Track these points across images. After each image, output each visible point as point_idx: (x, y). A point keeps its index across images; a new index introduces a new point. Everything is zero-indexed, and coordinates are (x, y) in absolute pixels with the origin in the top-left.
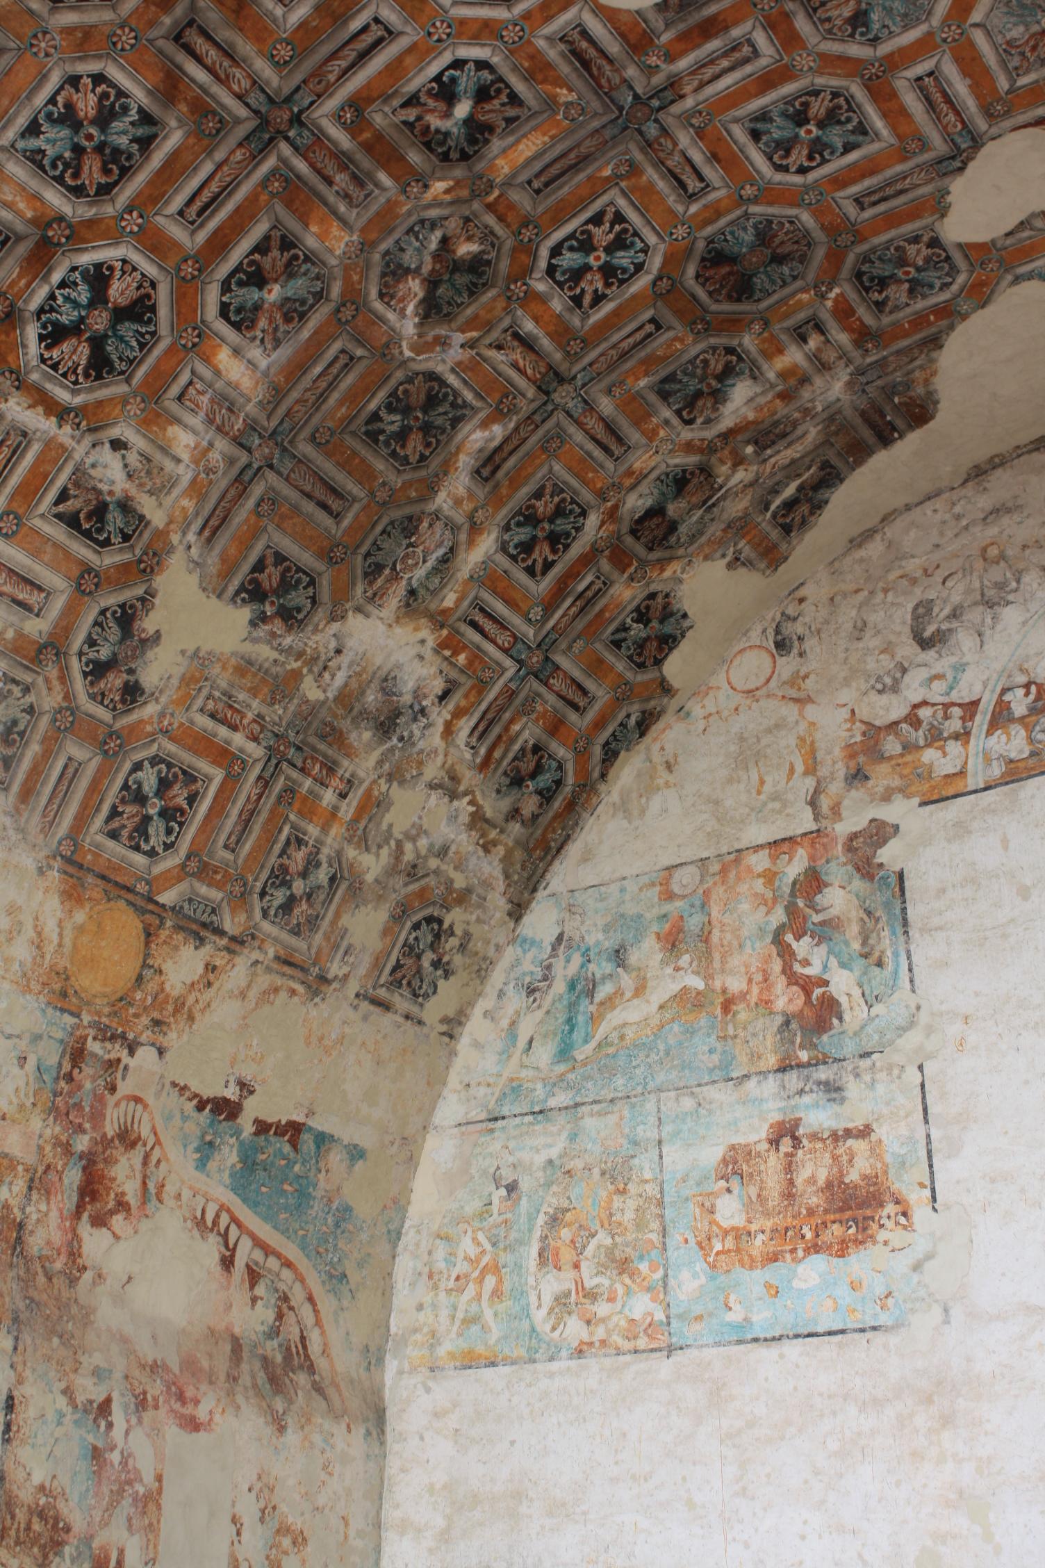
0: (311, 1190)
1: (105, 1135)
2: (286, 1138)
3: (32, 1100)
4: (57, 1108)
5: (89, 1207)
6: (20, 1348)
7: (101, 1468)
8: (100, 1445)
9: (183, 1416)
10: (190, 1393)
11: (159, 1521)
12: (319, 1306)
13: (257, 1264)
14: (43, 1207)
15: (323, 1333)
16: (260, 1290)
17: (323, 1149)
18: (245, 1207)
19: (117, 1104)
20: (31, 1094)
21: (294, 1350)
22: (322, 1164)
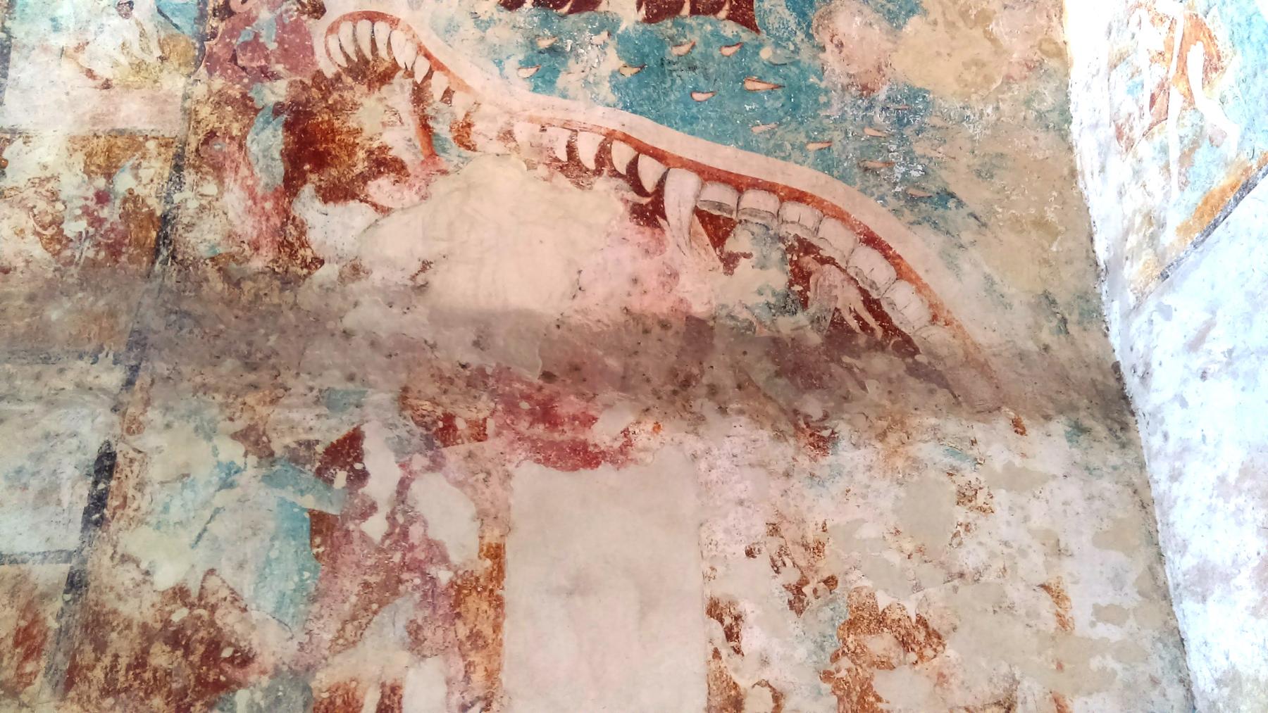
0: (813, 79)
1: (320, 73)
2: (723, 14)
3: (158, 53)
4: (211, 56)
5: (314, 177)
6: (143, 379)
7: (335, 548)
8: (332, 511)
9: (552, 444)
10: (569, 406)
11: (497, 628)
12: (897, 248)
13: (720, 206)
14: (210, 188)
15: (920, 288)
16: (739, 242)
17: (814, 16)
18: (664, 129)
19: (332, 29)
20: (154, 46)
21: (854, 324)
22: (823, 37)
